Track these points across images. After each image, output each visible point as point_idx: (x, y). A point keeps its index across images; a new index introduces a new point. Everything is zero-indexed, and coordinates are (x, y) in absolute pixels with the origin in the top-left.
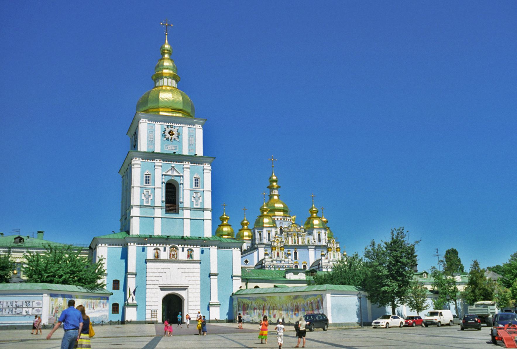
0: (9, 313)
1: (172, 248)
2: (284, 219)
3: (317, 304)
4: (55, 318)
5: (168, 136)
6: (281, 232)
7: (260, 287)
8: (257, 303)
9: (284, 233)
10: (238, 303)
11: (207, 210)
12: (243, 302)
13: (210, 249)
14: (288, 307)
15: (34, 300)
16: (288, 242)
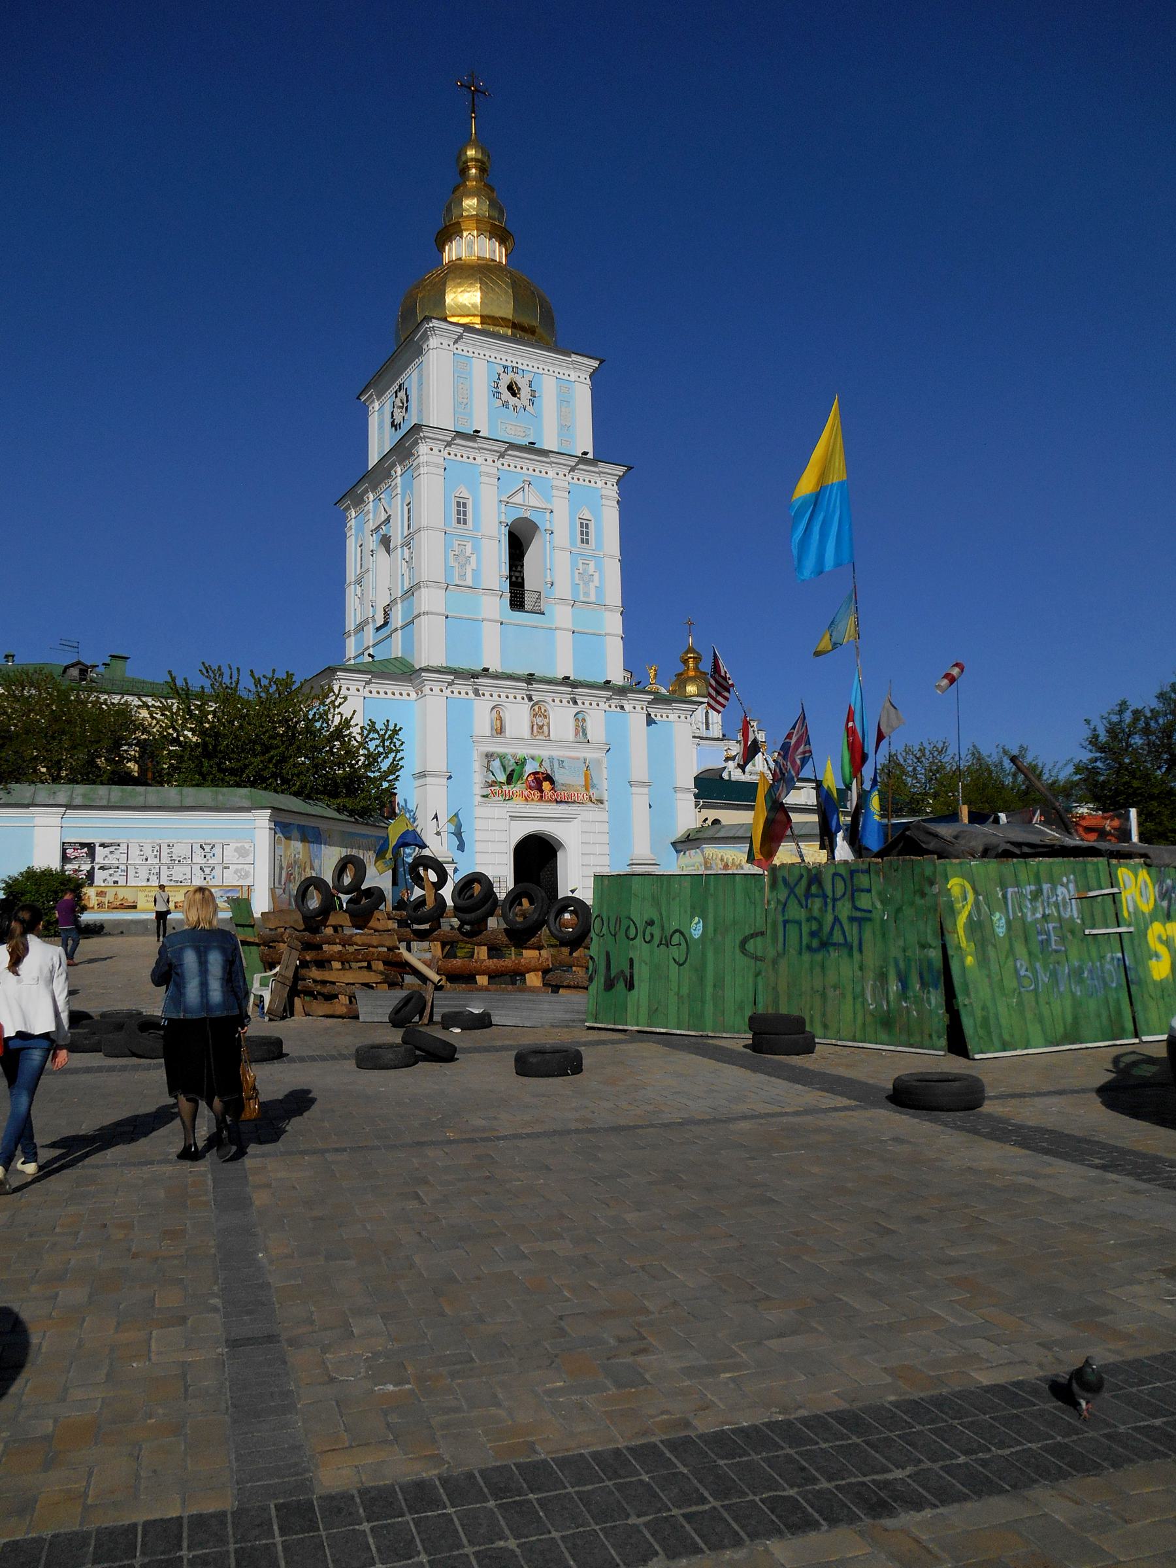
0: (148, 880)
4: (285, 897)
5: (506, 395)
7: (723, 823)
10: (706, 863)
12: (722, 860)
15: (225, 841)
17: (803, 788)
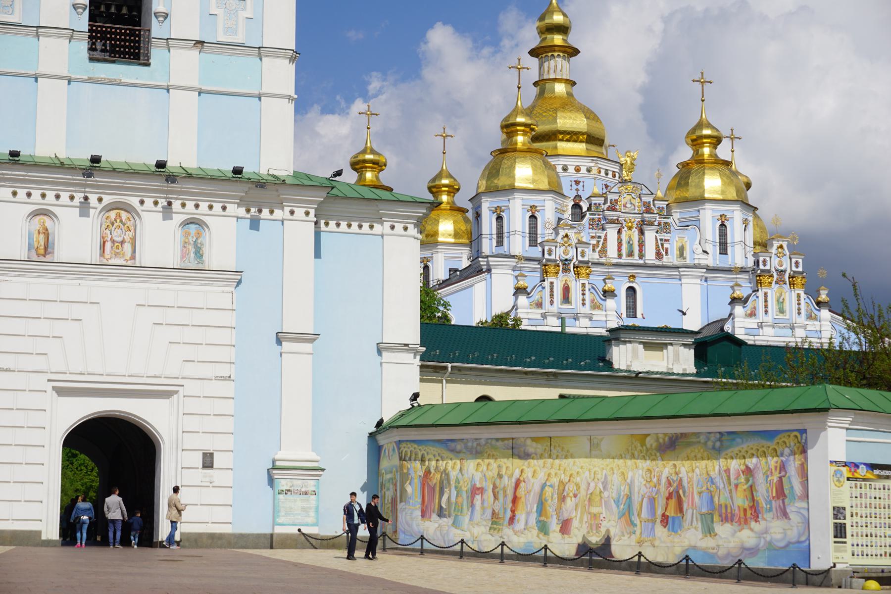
1: (113, 214)
2: (589, 170)
3: (775, 478)
6: (578, 212)
8: (485, 468)
9: (588, 216)
11: (276, 52)
13: (283, 224)
14: (631, 486)
16: (603, 252)
17: (666, 345)
